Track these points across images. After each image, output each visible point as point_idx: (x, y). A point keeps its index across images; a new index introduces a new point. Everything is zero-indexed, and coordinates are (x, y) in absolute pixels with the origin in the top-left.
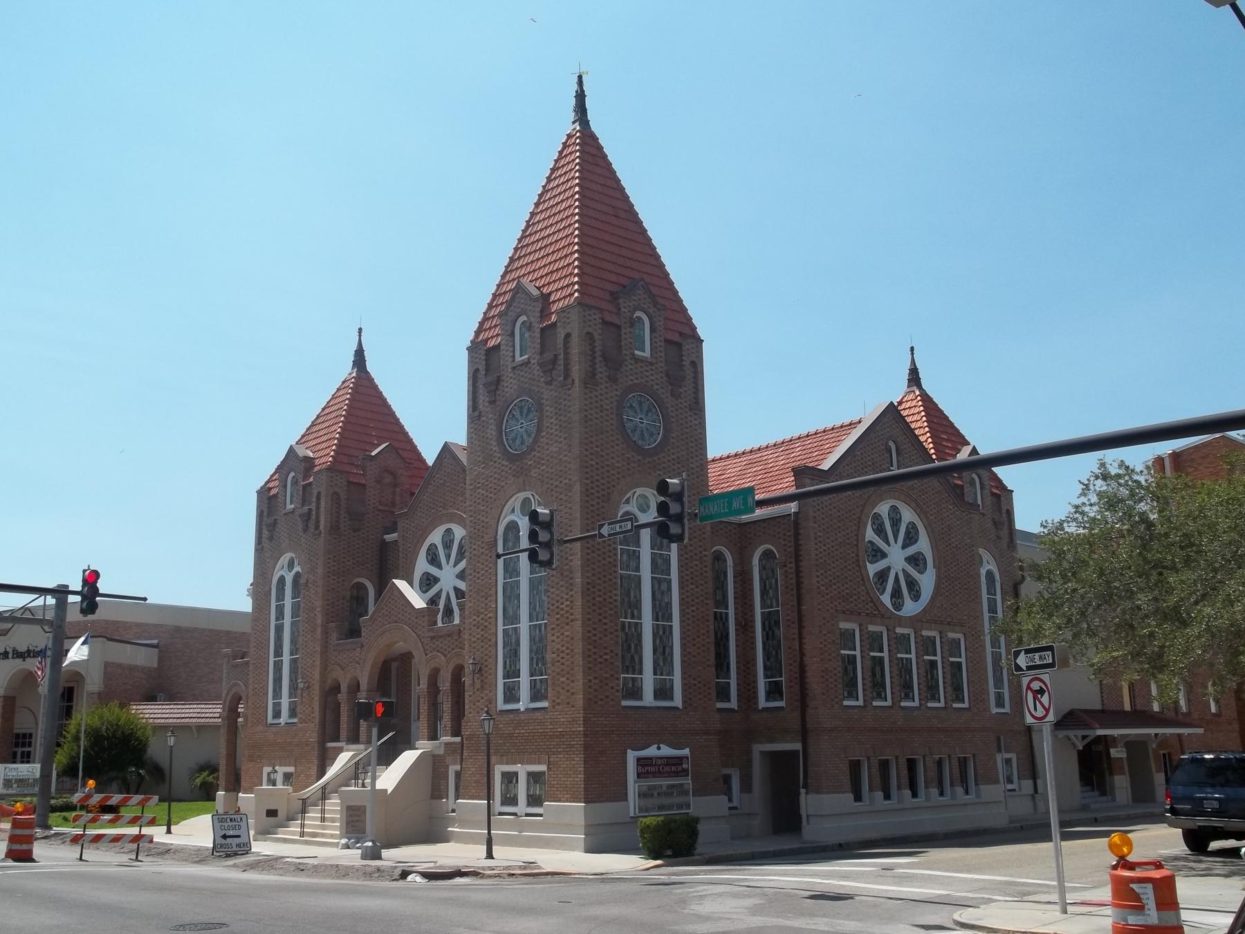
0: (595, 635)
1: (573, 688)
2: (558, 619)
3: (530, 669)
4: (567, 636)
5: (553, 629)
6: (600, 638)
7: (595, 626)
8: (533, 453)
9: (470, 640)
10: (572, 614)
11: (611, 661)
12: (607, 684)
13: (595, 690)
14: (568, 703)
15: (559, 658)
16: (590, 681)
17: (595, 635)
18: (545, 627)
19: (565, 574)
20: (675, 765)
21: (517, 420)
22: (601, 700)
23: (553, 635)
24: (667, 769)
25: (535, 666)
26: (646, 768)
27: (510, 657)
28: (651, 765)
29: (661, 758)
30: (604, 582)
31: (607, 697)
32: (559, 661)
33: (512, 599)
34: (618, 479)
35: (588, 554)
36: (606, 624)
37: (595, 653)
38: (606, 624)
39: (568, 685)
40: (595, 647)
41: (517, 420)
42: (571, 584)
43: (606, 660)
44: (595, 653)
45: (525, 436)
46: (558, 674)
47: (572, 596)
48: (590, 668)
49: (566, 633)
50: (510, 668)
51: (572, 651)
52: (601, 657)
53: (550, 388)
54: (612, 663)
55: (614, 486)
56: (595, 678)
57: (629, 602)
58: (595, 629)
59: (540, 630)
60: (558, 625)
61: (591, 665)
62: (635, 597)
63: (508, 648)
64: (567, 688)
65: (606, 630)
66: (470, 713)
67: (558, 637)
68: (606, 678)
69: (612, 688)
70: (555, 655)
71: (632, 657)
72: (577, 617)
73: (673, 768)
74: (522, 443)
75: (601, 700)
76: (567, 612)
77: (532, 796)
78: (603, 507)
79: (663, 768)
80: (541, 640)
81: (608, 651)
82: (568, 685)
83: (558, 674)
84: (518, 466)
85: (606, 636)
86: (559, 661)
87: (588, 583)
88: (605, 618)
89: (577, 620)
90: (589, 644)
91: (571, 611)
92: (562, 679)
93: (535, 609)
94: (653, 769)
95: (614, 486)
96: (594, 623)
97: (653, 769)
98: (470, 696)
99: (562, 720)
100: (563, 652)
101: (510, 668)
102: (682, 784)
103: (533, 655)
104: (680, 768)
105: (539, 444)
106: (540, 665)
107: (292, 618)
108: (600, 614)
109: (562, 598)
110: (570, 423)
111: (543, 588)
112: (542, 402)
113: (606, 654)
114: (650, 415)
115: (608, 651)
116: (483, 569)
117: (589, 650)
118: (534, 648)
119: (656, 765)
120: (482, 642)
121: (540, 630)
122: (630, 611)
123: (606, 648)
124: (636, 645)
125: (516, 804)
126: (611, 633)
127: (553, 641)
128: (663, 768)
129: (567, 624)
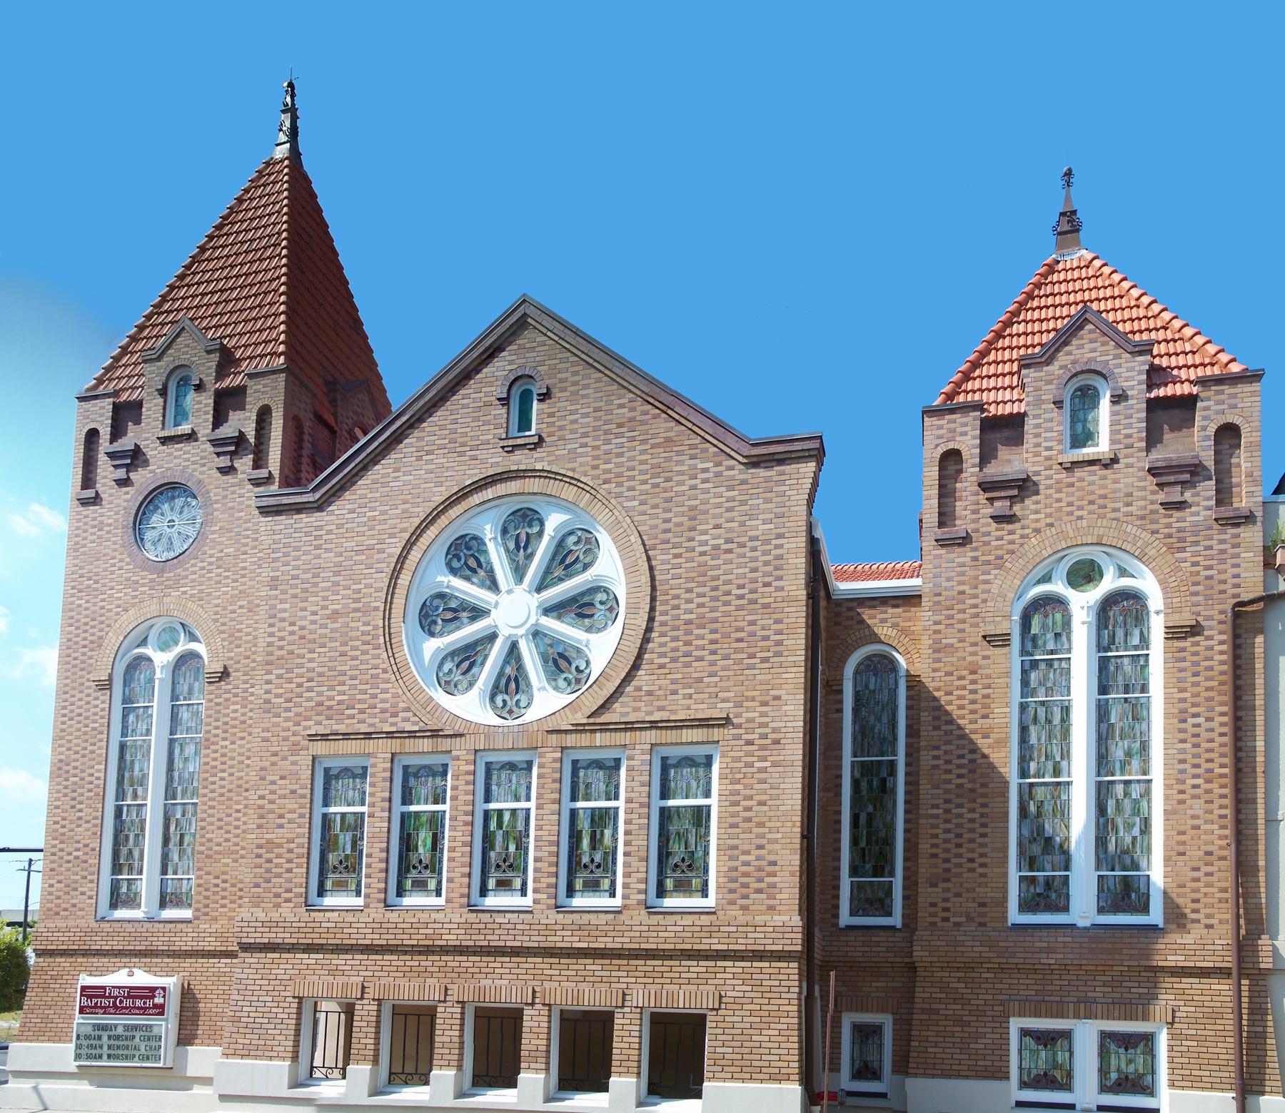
0: (64, 827)
6: (72, 830)
7: (64, 815)
11: (85, 857)
12: (76, 889)
13: (59, 898)
16: (51, 886)
17: (64, 827)
20: (141, 998)
22: (66, 910)
24: (129, 1002)
26: (94, 1001)
28: (104, 996)
29: (119, 988)
30: (84, 756)
31: (74, 905)
34: (117, 614)
35: (64, 723)
36: (81, 811)
37: (61, 850)
38: (81, 811)
40: (62, 842)
43: (77, 858)
44: (61, 850)
48: (52, 870)
52: (70, 854)
54: (86, 862)
55: (109, 626)
56: (59, 882)
57: (132, 778)
58: (64, 819)
61: (54, 865)
62: (141, 770)
65: (80, 818)
68: (76, 882)
69: (83, 893)
71: (130, 852)
73: (139, 1003)
75: (66, 910)
78: (90, 658)
79: (121, 1002)
81: (80, 845)
85: (79, 826)
87: (61, 761)
88: (81, 803)
90: (54, 839)
94: (105, 1002)
95: (109, 626)
96: (65, 811)
97: (105, 1002)
102: (151, 1026)
104: (149, 1003)
108: (74, 799)
113: (78, 850)
114: (186, 510)
115: (80, 845)
117: (54, 846)
119: (110, 997)
122: (131, 789)
123: (78, 842)
124: (137, 835)
126: (88, 822)
128: (121, 1002)
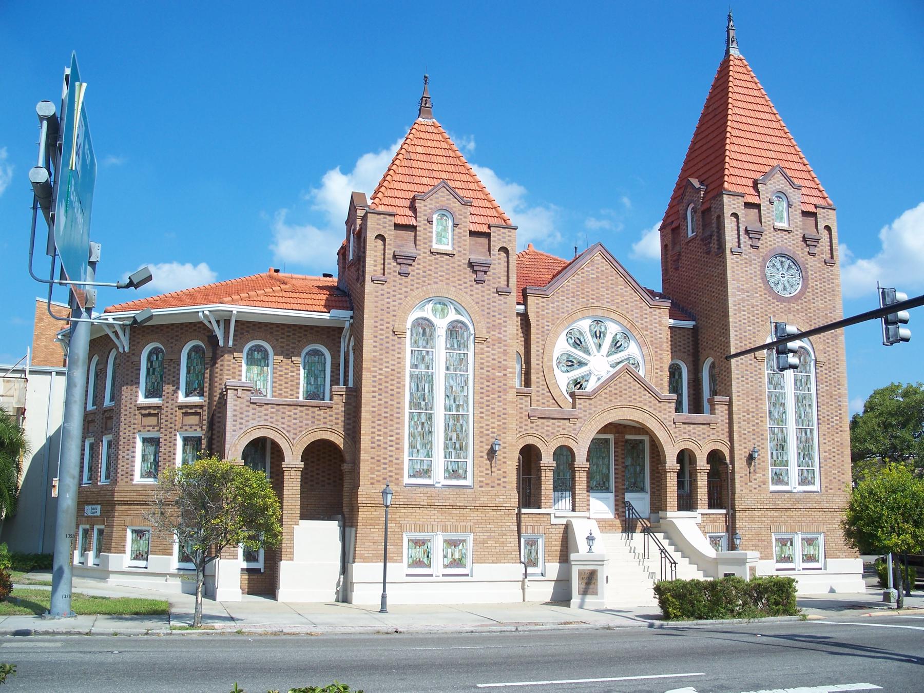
1: (843, 478)
2: (829, 428)
3: (798, 461)
4: (838, 442)
5: (824, 435)
8: (800, 301)
9: (740, 432)
10: (841, 427)
14: (839, 489)
15: (831, 456)
18: (811, 432)
19: (834, 397)
21: (778, 269)
23: (825, 439)
25: (802, 459)
27: (777, 450)
32: (830, 459)
33: (778, 406)
39: (839, 476)
41: (778, 269)
42: (840, 405)
45: (787, 285)
46: (830, 467)
47: (840, 414)
49: (836, 439)
50: (777, 458)
51: (842, 452)
53: (814, 258)
59: (806, 434)
60: (828, 433)
63: (775, 443)
64: (838, 478)
66: (742, 490)
67: (829, 441)
70: (827, 454)
72: (846, 429)
74: (785, 289)
76: (837, 424)
77: (806, 555)
80: (807, 441)
82: (839, 476)
83: (830, 467)
84: (785, 306)
86: (830, 459)
89: (845, 431)
91: (841, 424)
92: (833, 472)
93: (800, 418)
98: (741, 477)
99: (837, 500)
100: (834, 452)
101: (777, 458)
103: (800, 451)
105: (805, 296)
106: (807, 459)
107: (447, 369)
109: (832, 414)
110: (833, 291)
111: (806, 402)
112: (806, 266)
116: (752, 377)
118: (801, 446)
120: (754, 435)
121: (806, 434)
125: (792, 562)
127: (825, 443)
129: (837, 433)
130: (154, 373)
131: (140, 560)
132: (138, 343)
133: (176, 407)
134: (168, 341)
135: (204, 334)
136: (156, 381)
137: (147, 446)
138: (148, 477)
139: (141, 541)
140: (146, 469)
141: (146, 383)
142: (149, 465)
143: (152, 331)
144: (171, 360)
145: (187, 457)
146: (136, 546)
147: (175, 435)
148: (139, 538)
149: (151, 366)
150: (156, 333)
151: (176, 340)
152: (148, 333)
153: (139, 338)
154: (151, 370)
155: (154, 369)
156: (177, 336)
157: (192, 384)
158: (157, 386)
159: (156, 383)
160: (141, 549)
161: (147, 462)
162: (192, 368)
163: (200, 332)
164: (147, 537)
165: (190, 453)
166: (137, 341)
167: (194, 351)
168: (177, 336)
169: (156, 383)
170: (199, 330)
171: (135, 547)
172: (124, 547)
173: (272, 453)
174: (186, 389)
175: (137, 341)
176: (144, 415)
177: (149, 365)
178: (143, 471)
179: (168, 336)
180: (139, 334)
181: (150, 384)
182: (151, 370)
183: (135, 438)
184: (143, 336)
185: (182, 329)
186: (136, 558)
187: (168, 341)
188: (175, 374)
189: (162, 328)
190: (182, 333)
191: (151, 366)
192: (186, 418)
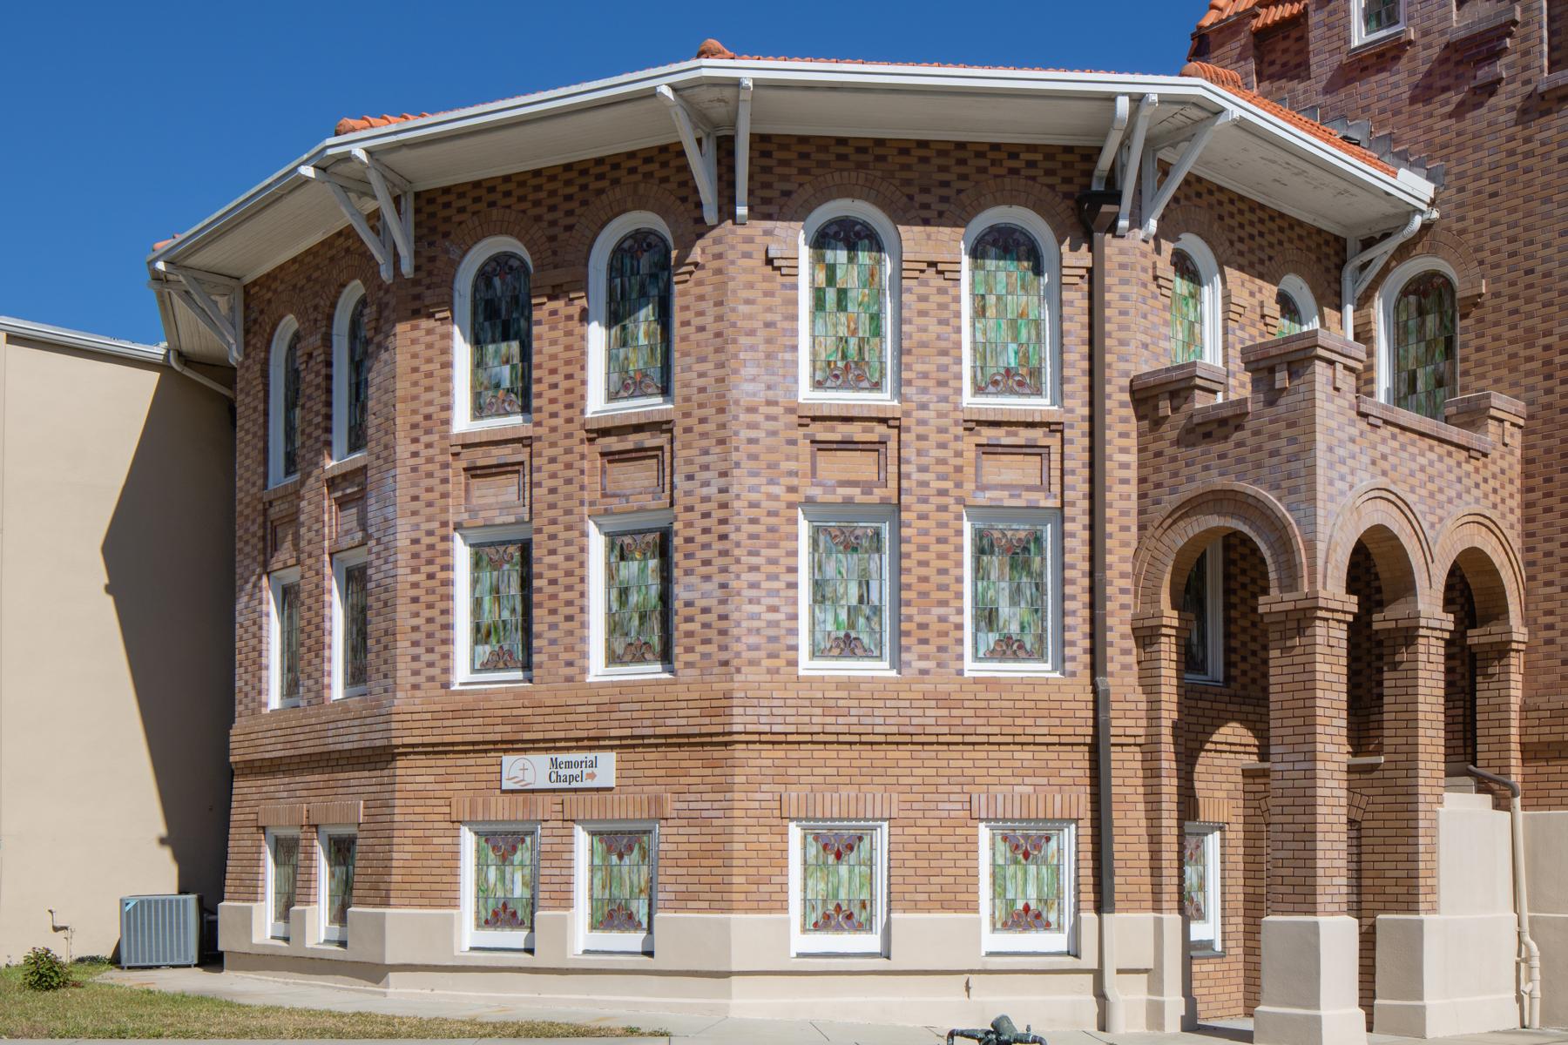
130: (841, 304)
131: (838, 928)
132: (787, 194)
133: (956, 423)
134: (911, 198)
135: (1052, 187)
136: (854, 332)
137: (829, 552)
138: (840, 656)
139: (843, 870)
140: (830, 627)
141: (814, 337)
142: (843, 616)
143: (842, 157)
144: (932, 264)
145: (991, 593)
146: (822, 886)
147: (959, 518)
148: (831, 859)
149: (831, 279)
150: (861, 166)
151: (944, 199)
152: (822, 164)
153: (785, 178)
154: (831, 295)
155: (842, 294)
156: (945, 184)
157: (996, 355)
158: (860, 350)
159: (853, 342)
160: (843, 895)
161: (835, 601)
162: (991, 300)
163: (1034, 178)
164: (864, 854)
165: (1001, 578)
166: (780, 186)
167: (994, 243)
168: (945, 184)
169: (853, 342)
170: (1032, 172)
171: (819, 887)
172: (784, 886)
173: (1228, 592)
174: (974, 367)
175: (780, 186)
176: (821, 445)
177: (821, 277)
178: (819, 636)
179: (908, 182)
180: (784, 163)
181: (831, 341)
182: (831, 295)
183: (795, 522)
184: (804, 171)
185: (962, 162)
186: (825, 923)
187: (911, 198)
188: (945, 314)
189: (879, 151)
190: (963, 177)
191: (831, 279)
192: (989, 463)
